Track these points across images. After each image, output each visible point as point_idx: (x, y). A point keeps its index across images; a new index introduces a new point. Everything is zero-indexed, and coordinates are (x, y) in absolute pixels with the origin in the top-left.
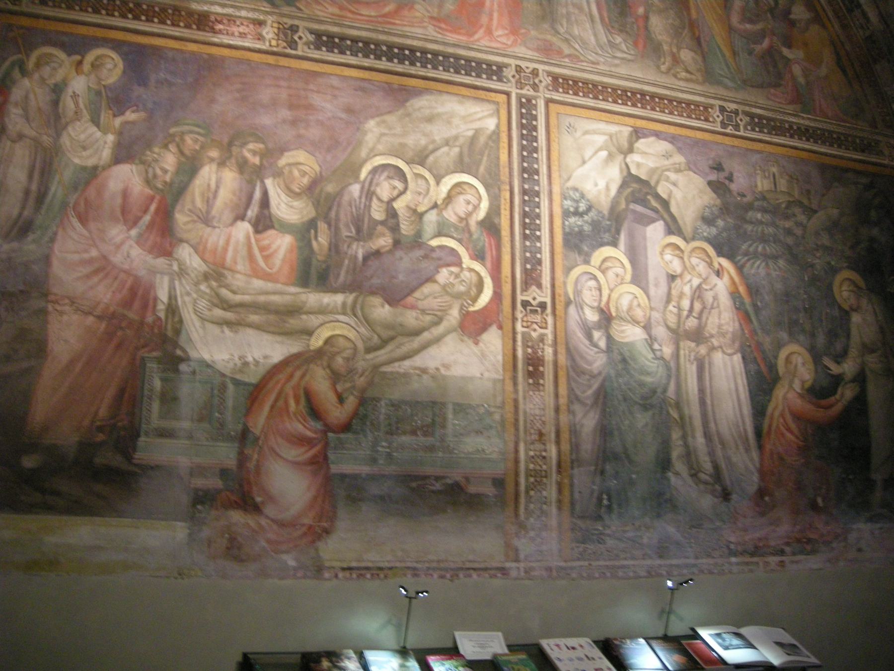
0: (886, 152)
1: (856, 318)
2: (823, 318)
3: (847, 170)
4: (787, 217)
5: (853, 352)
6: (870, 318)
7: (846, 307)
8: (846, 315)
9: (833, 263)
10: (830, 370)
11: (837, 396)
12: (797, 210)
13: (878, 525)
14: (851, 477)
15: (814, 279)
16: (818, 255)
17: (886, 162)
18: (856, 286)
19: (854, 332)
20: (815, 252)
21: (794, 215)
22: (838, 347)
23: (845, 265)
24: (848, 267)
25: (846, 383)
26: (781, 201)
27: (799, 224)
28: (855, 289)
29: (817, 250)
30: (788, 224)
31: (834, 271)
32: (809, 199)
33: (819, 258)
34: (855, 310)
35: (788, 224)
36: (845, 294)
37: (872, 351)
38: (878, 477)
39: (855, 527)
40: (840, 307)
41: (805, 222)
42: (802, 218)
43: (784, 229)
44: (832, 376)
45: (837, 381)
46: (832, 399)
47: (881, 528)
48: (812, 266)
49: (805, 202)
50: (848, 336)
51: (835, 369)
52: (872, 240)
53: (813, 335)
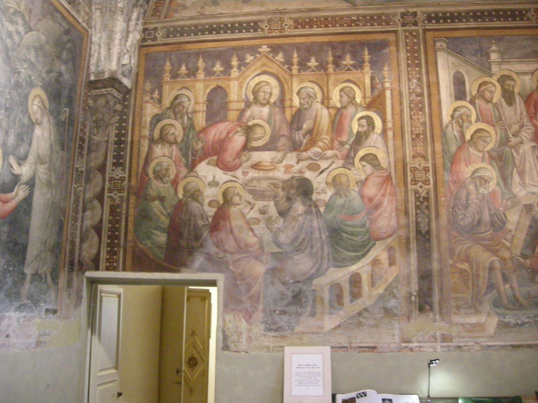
0: (82, 13)
1: (38, 131)
2: (17, 121)
3: (58, 11)
4: (12, 22)
5: (31, 158)
6: (46, 134)
7: (34, 121)
8: (32, 124)
9: (33, 78)
10: (13, 169)
11: (14, 193)
12: (20, 21)
13: (23, 314)
14: (11, 269)
15: (18, 85)
16: (25, 66)
17: (80, 20)
18: (44, 105)
19: (35, 142)
20: (24, 62)
21: (17, 24)
22: (22, 150)
23: (40, 84)
24: (41, 87)
25: (21, 184)
26: (11, 5)
27: (18, 33)
28: (42, 106)
29: (25, 61)
30: (11, 28)
31: (32, 85)
32: (30, 17)
33: (25, 69)
34: (39, 124)
35: (11, 28)
36: (35, 108)
37: (43, 163)
38: (28, 271)
39: (7, 314)
40: (29, 117)
41: (23, 33)
42: (21, 29)
43: (7, 30)
44: (14, 175)
45: (16, 179)
46: (10, 195)
47: (24, 317)
48: (19, 73)
49: (27, 18)
50: (30, 145)
51: (17, 170)
52: (60, 74)
53: (7, 133)
